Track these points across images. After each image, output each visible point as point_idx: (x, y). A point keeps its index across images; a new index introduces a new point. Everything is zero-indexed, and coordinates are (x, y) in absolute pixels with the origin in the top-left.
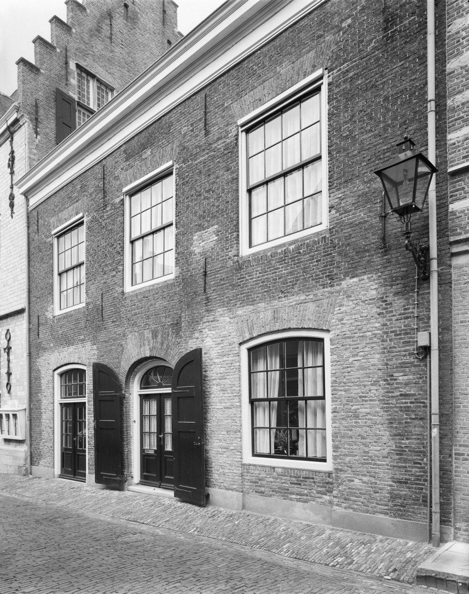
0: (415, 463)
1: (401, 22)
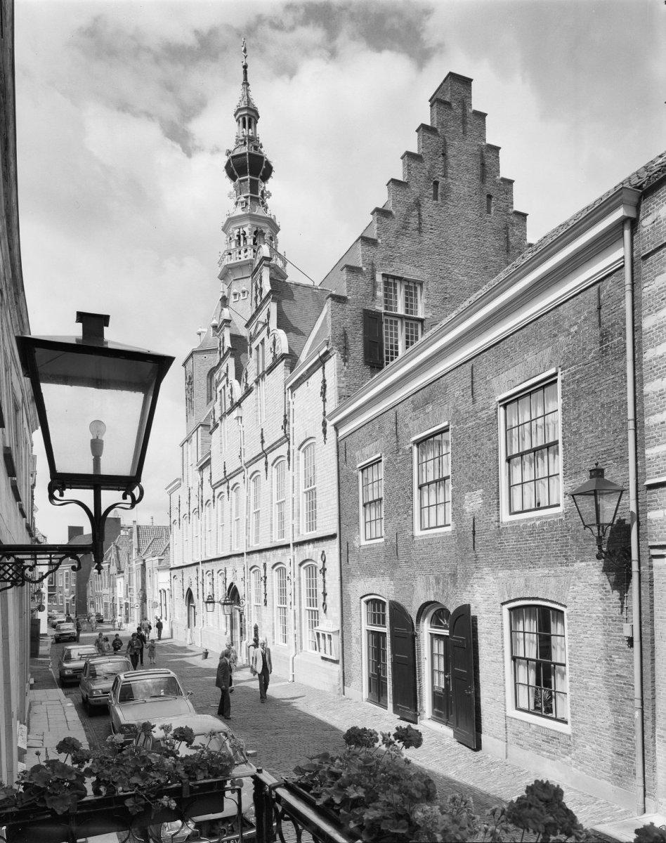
0: (628, 739)
1: (612, 340)
